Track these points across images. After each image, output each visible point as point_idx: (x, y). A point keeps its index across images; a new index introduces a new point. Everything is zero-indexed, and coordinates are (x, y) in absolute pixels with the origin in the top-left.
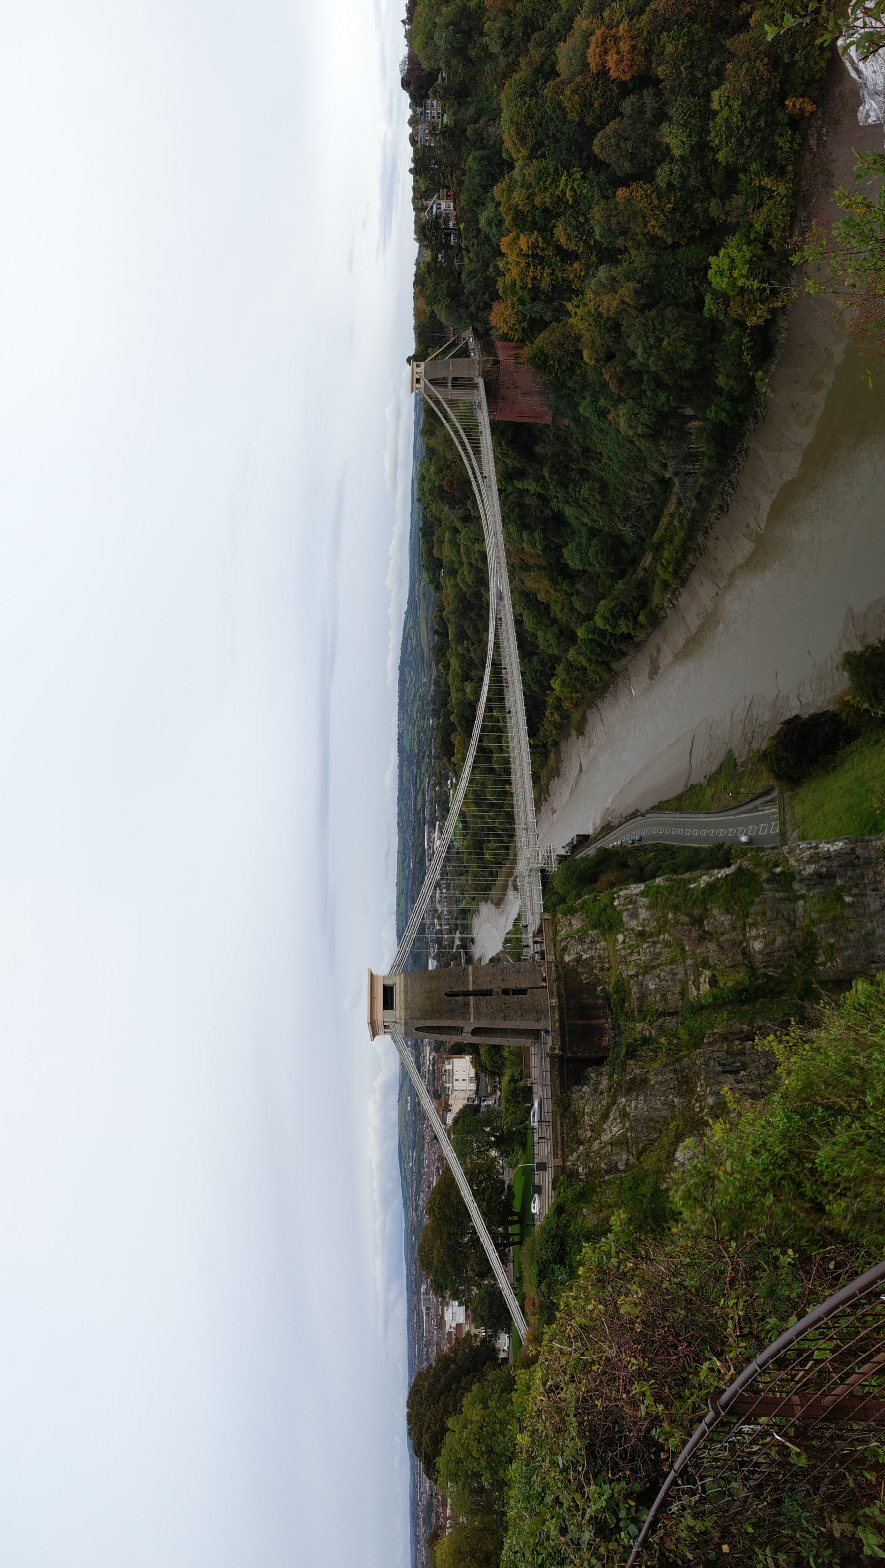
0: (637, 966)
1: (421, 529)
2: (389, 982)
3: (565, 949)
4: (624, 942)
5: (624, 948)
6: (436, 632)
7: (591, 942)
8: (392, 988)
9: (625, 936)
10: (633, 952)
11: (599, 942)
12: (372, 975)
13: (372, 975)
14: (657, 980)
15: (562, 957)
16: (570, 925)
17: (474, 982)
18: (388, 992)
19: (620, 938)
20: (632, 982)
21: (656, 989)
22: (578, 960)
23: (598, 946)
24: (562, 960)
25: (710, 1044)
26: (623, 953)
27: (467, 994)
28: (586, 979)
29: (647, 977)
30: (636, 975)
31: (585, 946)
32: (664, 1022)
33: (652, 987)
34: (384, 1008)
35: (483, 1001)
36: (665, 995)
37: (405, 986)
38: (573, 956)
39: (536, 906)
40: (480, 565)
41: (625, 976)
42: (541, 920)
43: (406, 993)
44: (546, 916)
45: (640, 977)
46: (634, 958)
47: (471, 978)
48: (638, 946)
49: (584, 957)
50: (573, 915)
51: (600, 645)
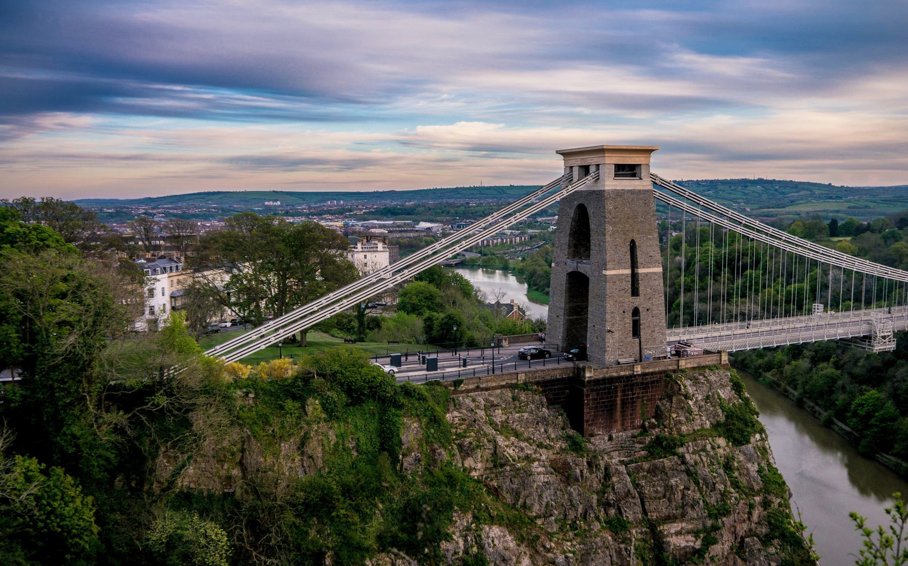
0: (696, 463)
2: (644, 173)
3: (696, 381)
5: (713, 448)
6: (834, 222)
8: (634, 175)
12: (653, 150)
13: (653, 150)
14: (682, 487)
16: (723, 386)
17: (647, 274)
20: (676, 458)
21: (672, 487)
22: (686, 397)
25: (619, 552)
26: (709, 447)
27: (634, 265)
29: (684, 476)
30: (684, 462)
31: (703, 403)
32: (634, 498)
35: (629, 286)
36: (664, 497)
38: (691, 390)
41: (681, 450)
42: (719, 352)
43: (632, 192)
44: (725, 358)
45: (683, 467)
46: (704, 459)
49: (691, 403)
50: (733, 389)
51: (869, 415)
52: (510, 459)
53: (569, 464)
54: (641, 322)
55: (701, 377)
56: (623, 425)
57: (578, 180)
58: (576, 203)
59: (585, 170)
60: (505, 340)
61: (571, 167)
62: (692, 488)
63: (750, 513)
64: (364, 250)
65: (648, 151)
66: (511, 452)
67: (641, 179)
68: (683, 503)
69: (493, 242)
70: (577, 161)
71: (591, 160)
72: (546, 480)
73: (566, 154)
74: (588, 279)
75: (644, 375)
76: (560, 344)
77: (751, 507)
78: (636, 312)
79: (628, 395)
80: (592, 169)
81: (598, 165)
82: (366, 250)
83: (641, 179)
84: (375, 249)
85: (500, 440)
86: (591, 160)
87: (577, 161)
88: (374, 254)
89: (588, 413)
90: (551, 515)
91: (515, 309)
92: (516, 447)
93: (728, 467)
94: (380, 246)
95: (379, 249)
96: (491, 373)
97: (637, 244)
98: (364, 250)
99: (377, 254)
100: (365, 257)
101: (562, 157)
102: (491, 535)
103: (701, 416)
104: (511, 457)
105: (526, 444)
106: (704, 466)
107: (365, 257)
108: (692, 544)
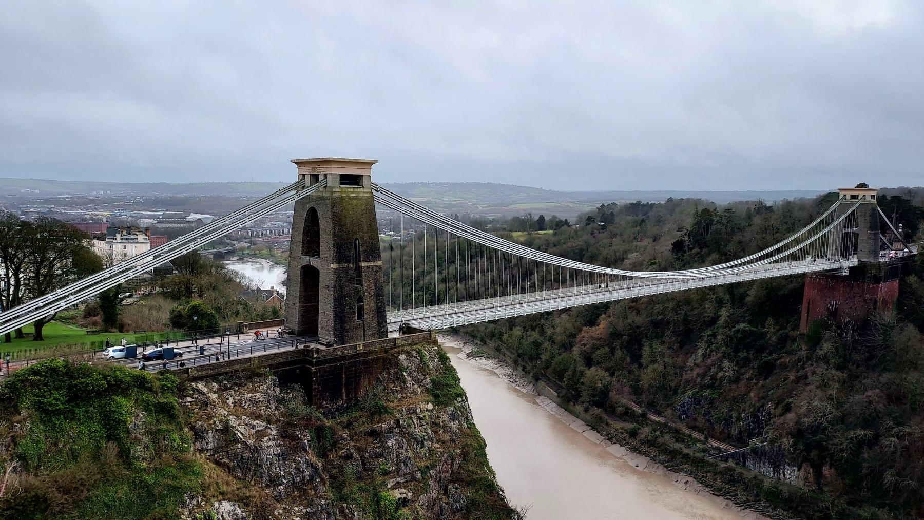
1: (639, 202)
2: (365, 182)
3: (408, 354)
4: (427, 410)
6: (542, 218)
7: (419, 379)
9: (431, 411)
10: (421, 419)
11: (419, 386)
15: (403, 352)
17: (368, 267)
18: (355, 180)
19: (430, 406)
21: (388, 447)
23: (416, 386)
24: (399, 353)
26: (418, 411)
28: (383, 377)
33: (389, 443)
37: (362, 199)
38: (405, 363)
39: (429, 324)
40: (627, 262)
42: (429, 330)
43: (356, 198)
45: (398, 430)
46: (415, 421)
48: (427, 424)
52: (241, 437)
53: (298, 436)
54: (365, 307)
55: (414, 352)
56: (347, 396)
57: (311, 186)
58: (308, 206)
59: (315, 177)
60: (246, 326)
61: (304, 175)
62: (405, 447)
63: (452, 464)
64: (123, 241)
65: (370, 164)
66: (242, 431)
67: (363, 187)
68: (397, 461)
69: (262, 233)
70: (308, 171)
71: (321, 170)
72: (276, 453)
73: (299, 163)
74: (319, 271)
75: (367, 354)
76: (296, 328)
77: (453, 459)
79: (352, 371)
80: (321, 178)
81: (326, 175)
82: (126, 241)
83: (363, 187)
84: (135, 240)
85: (233, 421)
86: (321, 170)
87: (308, 171)
88: (134, 245)
89: (315, 388)
90: (281, 485)
91: (275, 295)
92: (247, 425)
93: (435, 425)
95: (138, 241)
96: (226, 359)
98: (123, 241)
99: (137, 245)
100: (125, 248)
102: (221, 511)
103: (413, 384)
104: (242, 434)
105: (258, 422)
106: (415, 427)
107: (125, 248)
108: (404, 496)
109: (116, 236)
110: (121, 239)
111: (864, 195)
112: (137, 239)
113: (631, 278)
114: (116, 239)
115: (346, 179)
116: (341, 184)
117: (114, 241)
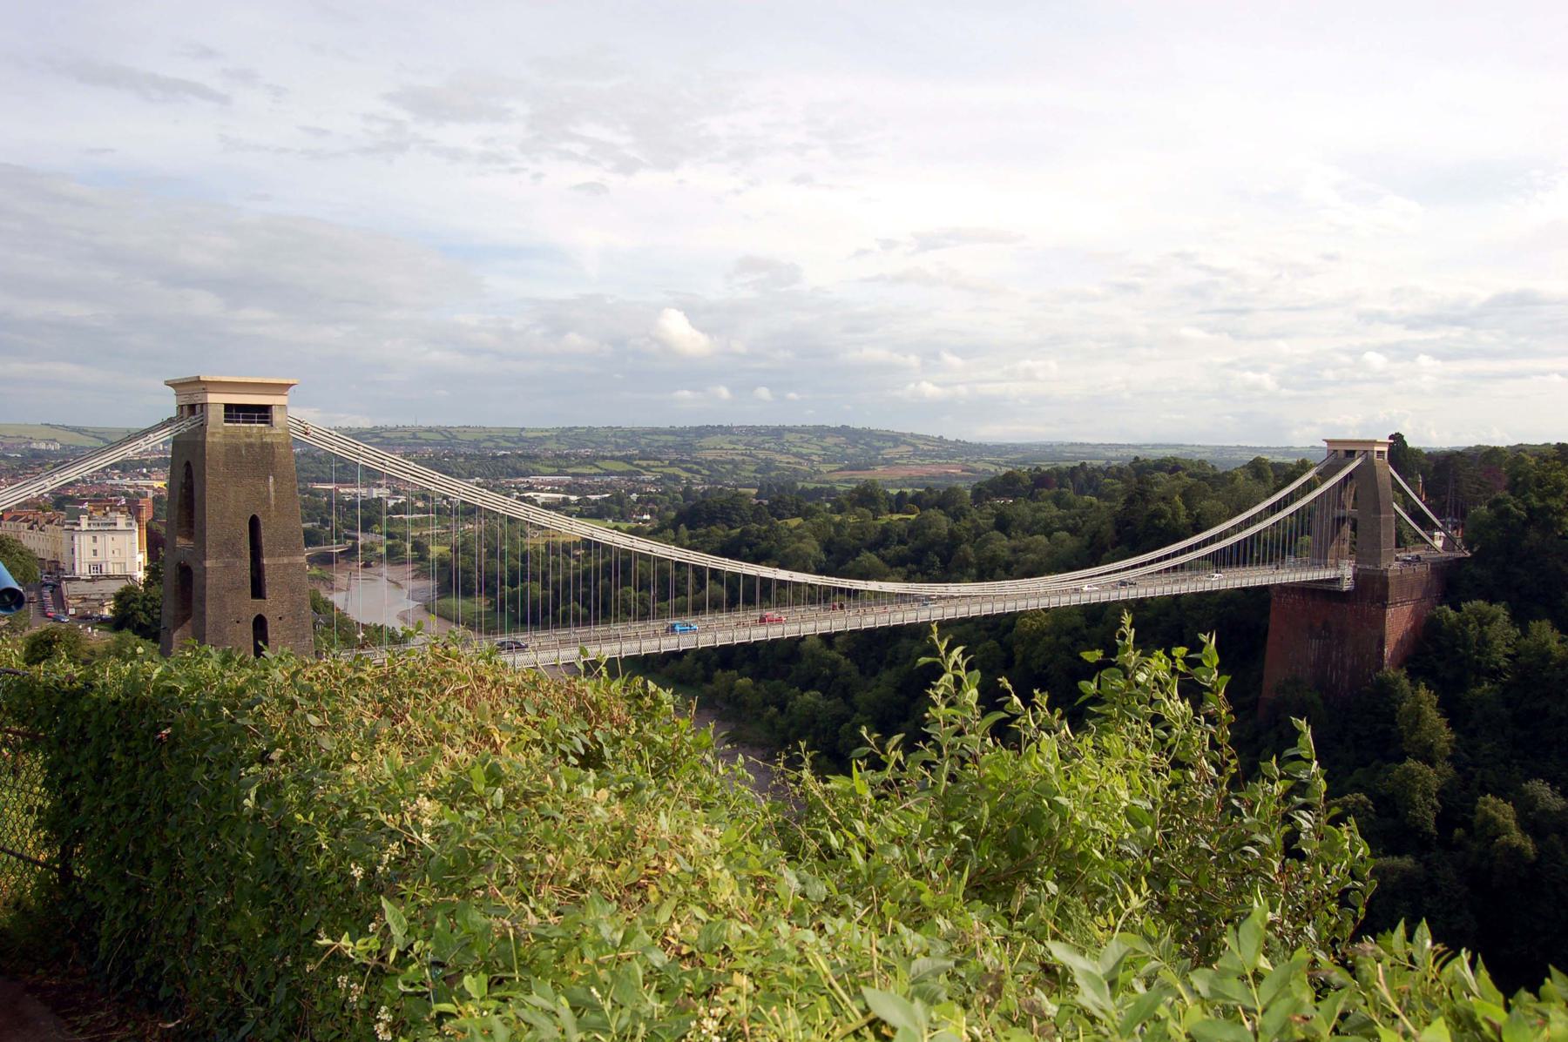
1: (1083, 465)
2: (277, 416)
18: (263, 412)
34: (228, 407)
47: (286, 560)
58: (184, 461)
64: (92, 528)
78: (260, 625)
80: (198, 408)
84: (111, 527)
88: (109, 537)
94: (121, 521)
95: (118, 527)
97: (262, 520)
99: (118, 537)
101: (172, 390)
109: (79, 519)
110: (89, 525)
111: (1366, 451)
112: (115, 524)
113: (853, 594)
114: (79, 525)
115: (233, 411)
116: (226, 422)
117: (77, 528)
